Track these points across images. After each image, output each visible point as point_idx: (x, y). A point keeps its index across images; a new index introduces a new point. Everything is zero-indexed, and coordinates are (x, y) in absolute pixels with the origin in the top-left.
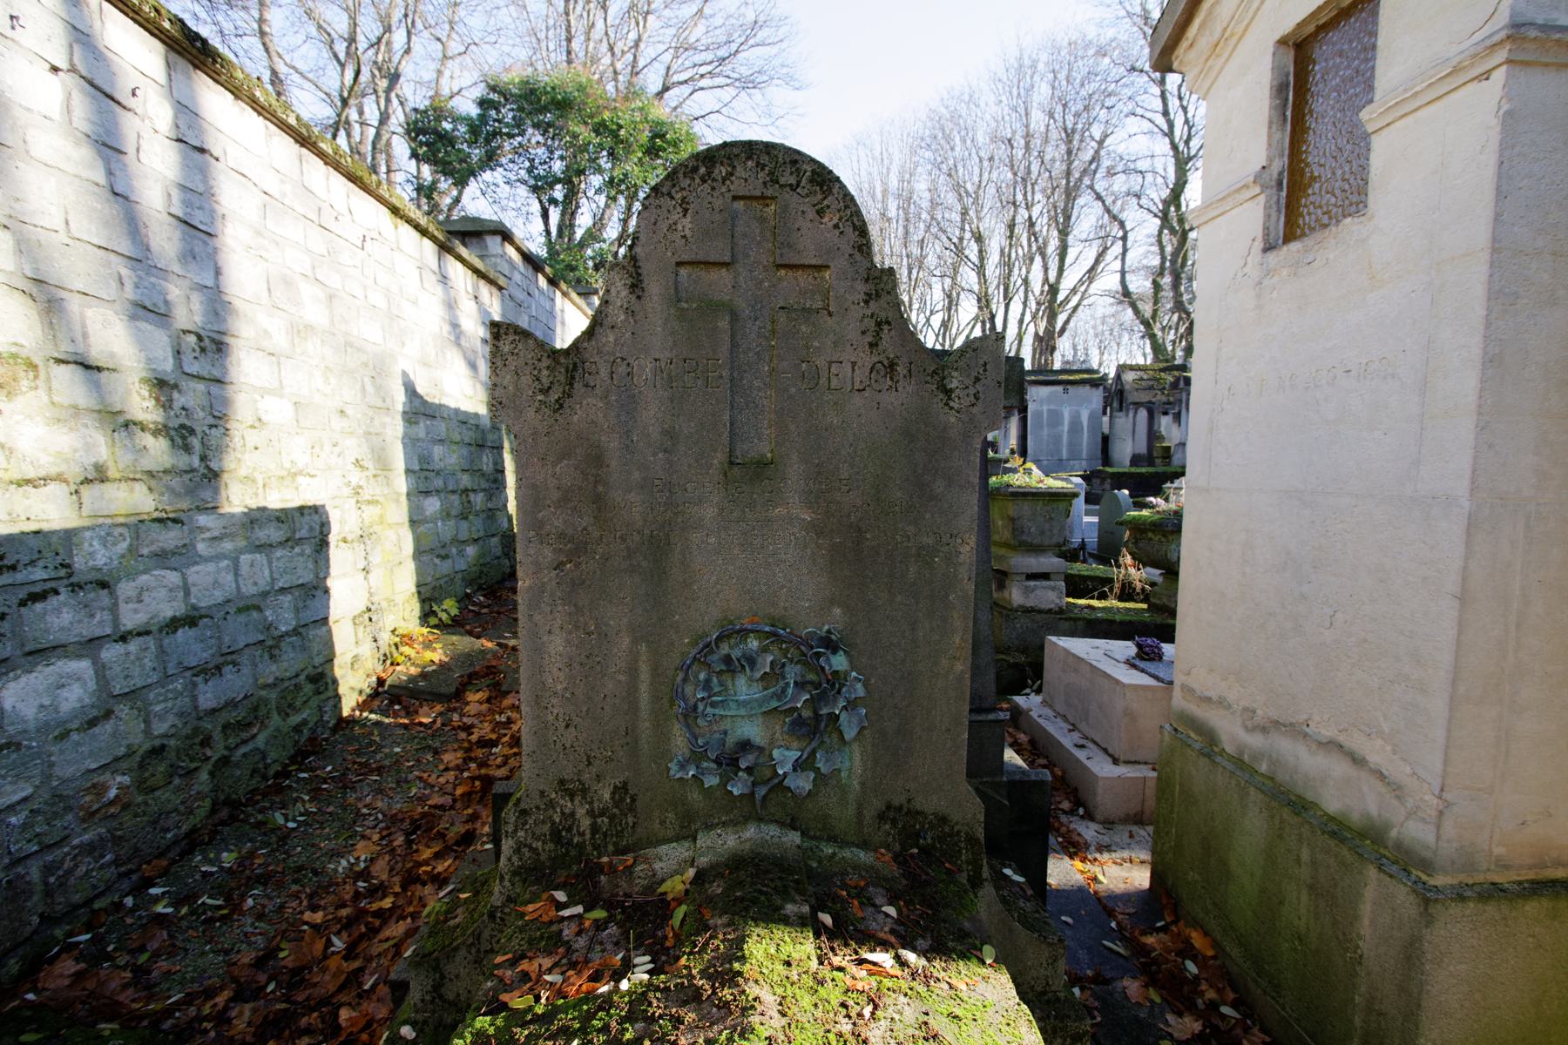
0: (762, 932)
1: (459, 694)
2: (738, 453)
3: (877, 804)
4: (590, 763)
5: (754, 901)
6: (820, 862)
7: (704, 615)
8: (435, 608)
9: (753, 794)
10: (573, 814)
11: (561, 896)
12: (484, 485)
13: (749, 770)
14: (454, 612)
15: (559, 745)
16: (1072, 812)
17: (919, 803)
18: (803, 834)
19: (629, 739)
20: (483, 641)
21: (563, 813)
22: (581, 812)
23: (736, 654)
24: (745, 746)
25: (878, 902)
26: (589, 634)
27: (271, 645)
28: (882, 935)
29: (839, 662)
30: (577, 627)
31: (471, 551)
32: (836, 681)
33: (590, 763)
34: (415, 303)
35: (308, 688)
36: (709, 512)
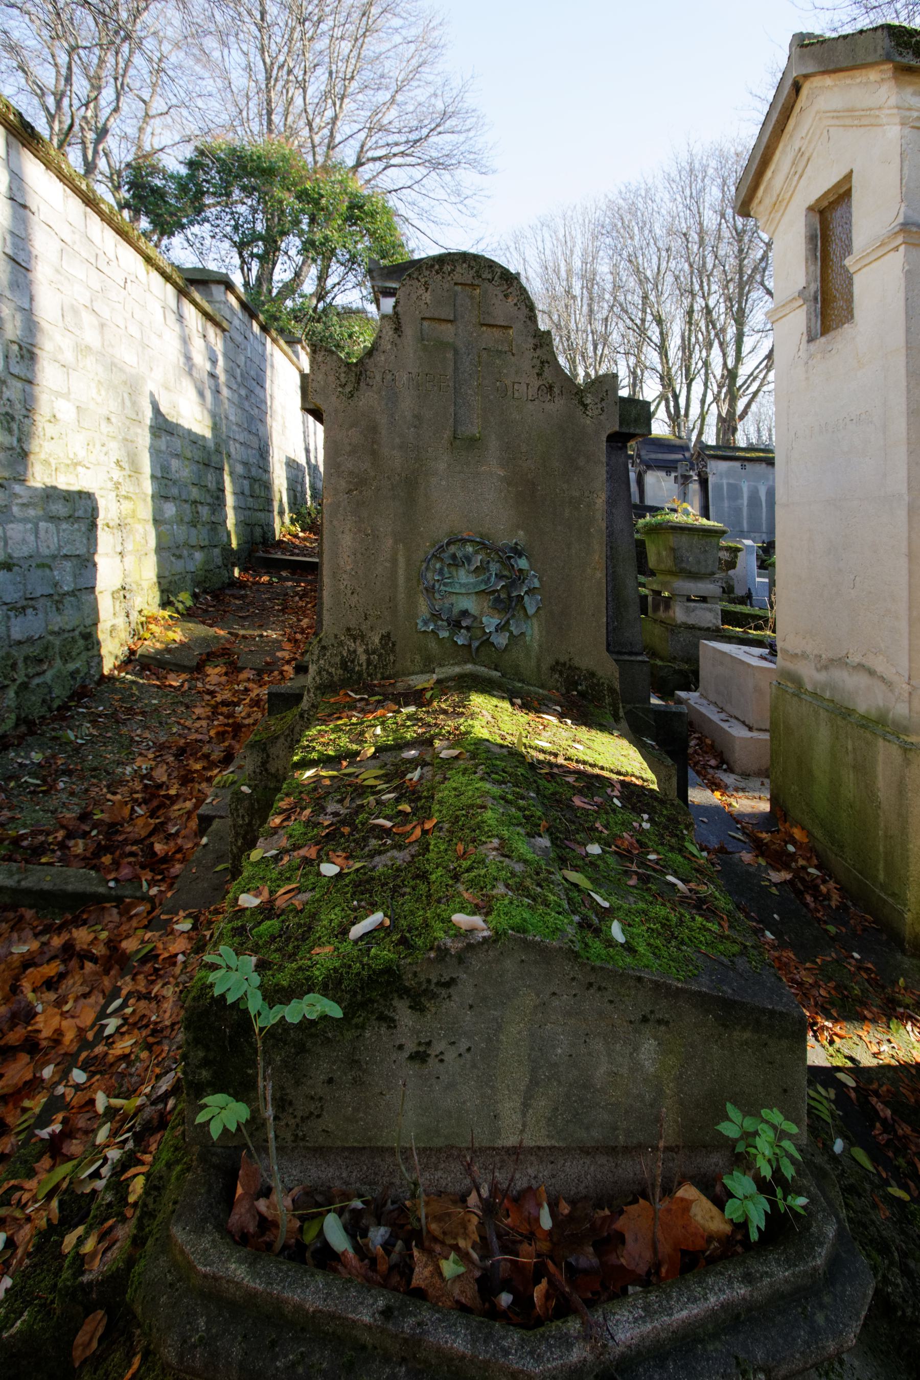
3: (548, 661)
9: (470, 645)
10: (355, 651)
13: (468, 628)
17: (577, 662)
22: (360, 650)
23: (459, 554)
24: (465, 613)
26: (367, 535)
27: (57, 600)
30: (360, 531)
34: (160, 336)
35: (81, 642)
36: (442, 466)
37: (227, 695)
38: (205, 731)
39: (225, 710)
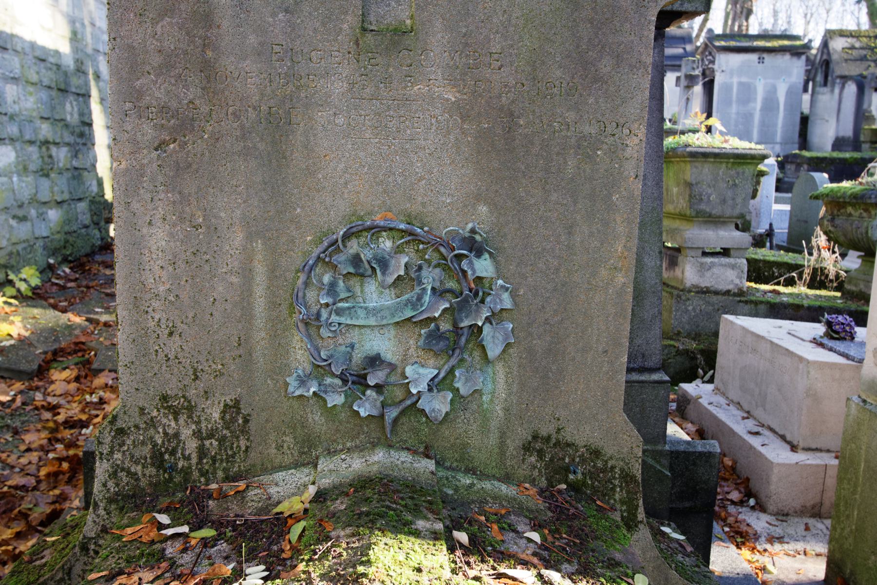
0: (390, 542)
1: (42, 372)
2: (372, 18)
3: (522, 434)
4: (197, 378)
5: (382, 516)
6: (456, 490)
7: (330, 210)
8: (12, 276)
9: (382, 416)
10: (177, 435)
11: (164, 519)
12: (69, 138)
13: (378, 388)
14: (35, 281)
15: (161, 355)
16: (742, 503)
17: (568, 435)
18: (438, 463)
19: (241, 351)
20: (70, 315)
21: (166, 434)
22: (186, 433)
23: (366, 255)
24: (374, 361)
25: (519, 529)
26: (196, 227)
28: (523, 556)
29: (483, 267)
30: (182, 219)
31: (54, 215)
32: (479, 290)
33: (197, 378)
37: (74, 411)
38: (32, 469)
39: (67, 434)
